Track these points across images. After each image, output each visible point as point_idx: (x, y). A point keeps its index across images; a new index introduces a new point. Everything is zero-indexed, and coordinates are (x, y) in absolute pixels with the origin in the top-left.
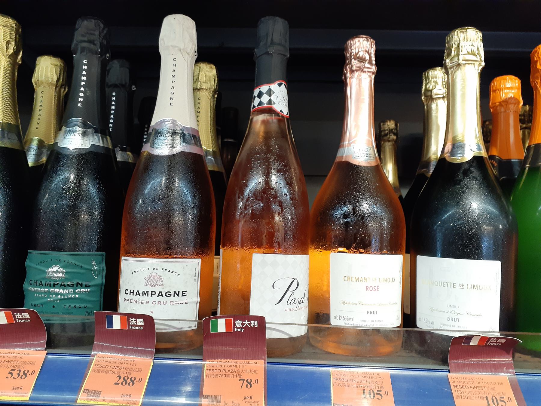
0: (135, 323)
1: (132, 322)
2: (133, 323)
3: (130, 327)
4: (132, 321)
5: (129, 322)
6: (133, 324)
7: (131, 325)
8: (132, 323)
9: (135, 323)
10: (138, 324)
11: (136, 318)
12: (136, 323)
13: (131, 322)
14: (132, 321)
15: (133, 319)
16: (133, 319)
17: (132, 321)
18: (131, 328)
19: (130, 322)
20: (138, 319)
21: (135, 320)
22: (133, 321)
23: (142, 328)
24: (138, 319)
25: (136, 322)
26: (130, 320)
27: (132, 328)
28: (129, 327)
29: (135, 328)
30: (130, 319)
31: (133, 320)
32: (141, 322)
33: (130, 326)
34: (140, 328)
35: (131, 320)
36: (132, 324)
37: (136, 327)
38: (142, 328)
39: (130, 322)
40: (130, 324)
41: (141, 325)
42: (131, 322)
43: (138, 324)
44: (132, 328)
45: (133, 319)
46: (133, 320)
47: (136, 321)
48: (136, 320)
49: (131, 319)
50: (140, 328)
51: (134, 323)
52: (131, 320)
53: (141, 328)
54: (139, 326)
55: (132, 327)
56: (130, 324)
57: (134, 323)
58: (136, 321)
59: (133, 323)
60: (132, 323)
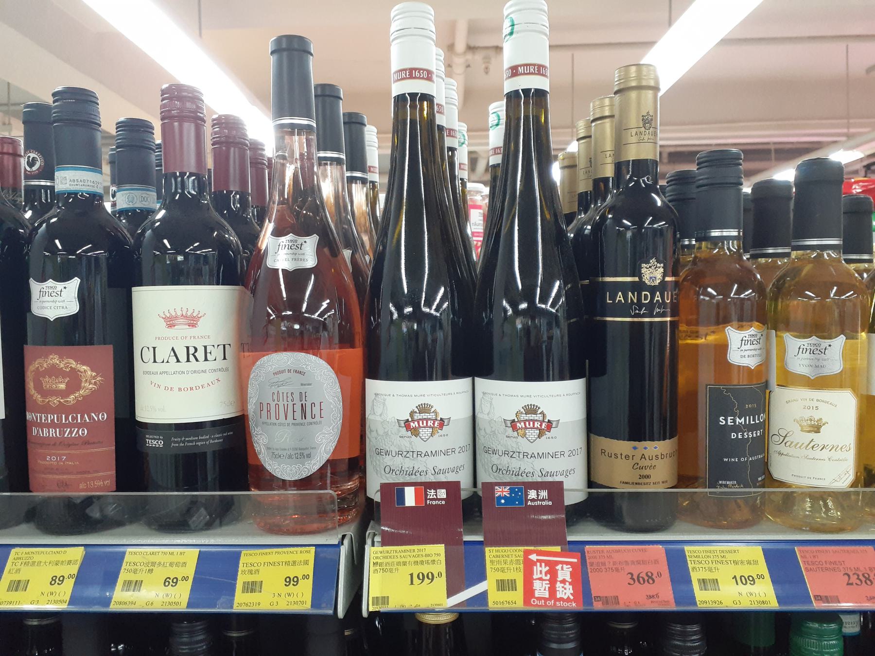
1: (430, 495)
2: (432, 496)
3: (428, 502)
5: (426, 495)
6: (431, 497)
7: (429, 499)
10: (438, 497)
11: (435, 489)
12: (436, 495)
14: (431, 493)
18: (429, 503)
19: (428, 494)
20: (438, 490)
21: (435, 491)
22: (432, 494)
23: (443, 502)
24: (438, 490)
26: (428, 493)
29: (434, 503)
30: (428, 490)
31: (431, 492)
32: (442, 493)
33: (428, 501)
35: (430, 492)
39: (428, 494)
40: (428, 498)
41: (442, 497)
43: (438, 497)
45: (432, 491)
46: (431, 492)
47: (435, 494)
48: (436, 492)
51: (433, 496)
52: (430, 492)
55: (431, 502)
57: (433, 496)
58: (435, 494)
59: (432, 496)
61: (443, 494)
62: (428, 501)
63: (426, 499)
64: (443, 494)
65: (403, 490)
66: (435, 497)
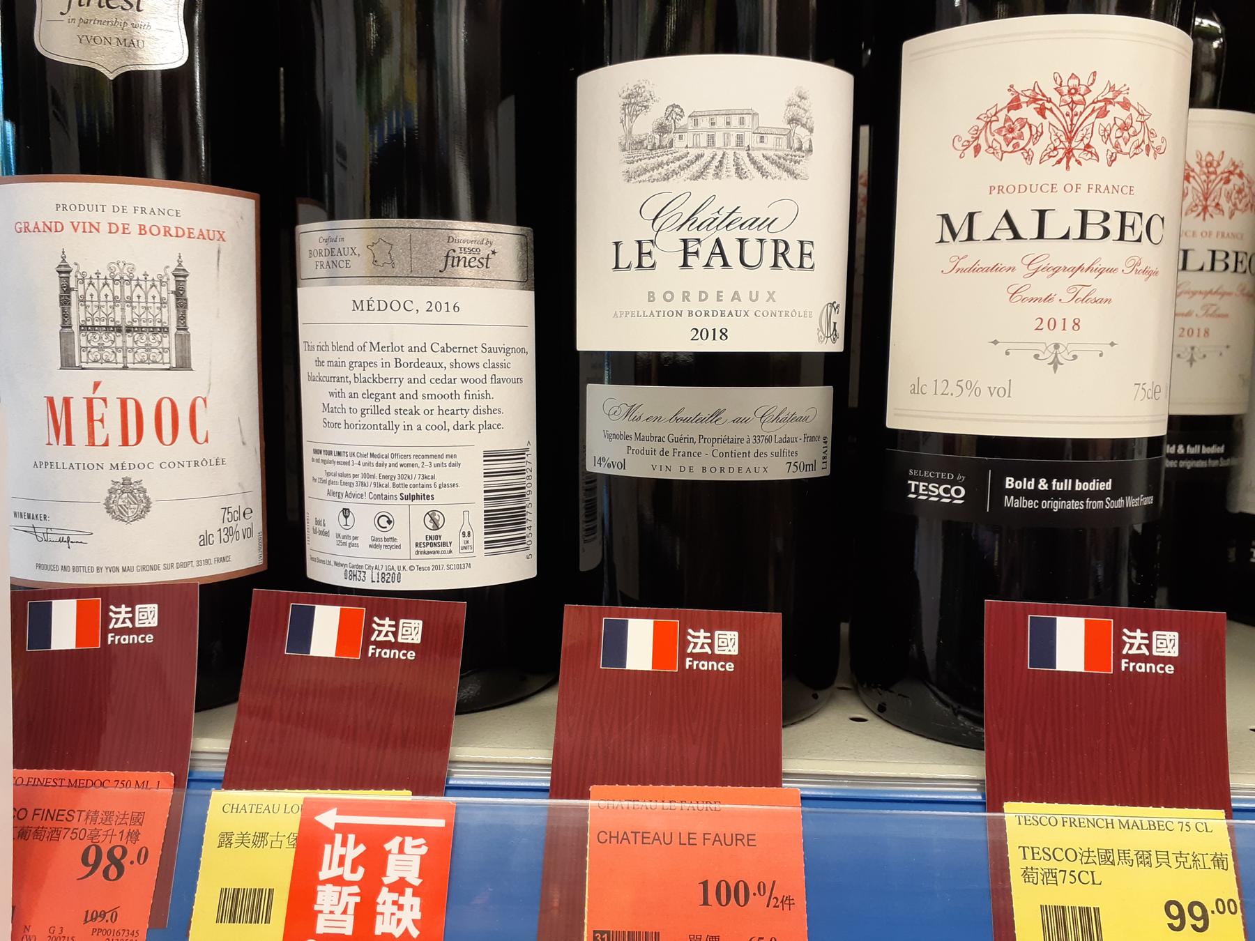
0: (1143, 647)
1: (1132, 645)
4: (1131, 641)
5: (1120, 644)
6: (1134, 651)
7: (1127, 656)
9: (1143, 647)
12: (1149, 647)
13: (1128, 646)
15: (1139, 630)
17: (1131, 641)
20: (1155, 633)
22: (1137, 642)
24: (1155, 633)
29: (1142, 668)
30: (1125, 631)
31: (1135, 638)
35: (1130, 637)
37: (1148, 665)
39: (1125, 643)
40: (1124, 652)
42: (1128, 646)
43: (1155, 653)
45: (1138, 633)
46: (1135, 638)
47: (1147, 642)
55: (1132, 664)
56: (1124, 652)
57: (1139, 648)
58: (1147, 642)
60: (1130, 648)
61: (1170, 645)
63: (1119, 656)
64: (1170, 645)
66: (1145, 651)
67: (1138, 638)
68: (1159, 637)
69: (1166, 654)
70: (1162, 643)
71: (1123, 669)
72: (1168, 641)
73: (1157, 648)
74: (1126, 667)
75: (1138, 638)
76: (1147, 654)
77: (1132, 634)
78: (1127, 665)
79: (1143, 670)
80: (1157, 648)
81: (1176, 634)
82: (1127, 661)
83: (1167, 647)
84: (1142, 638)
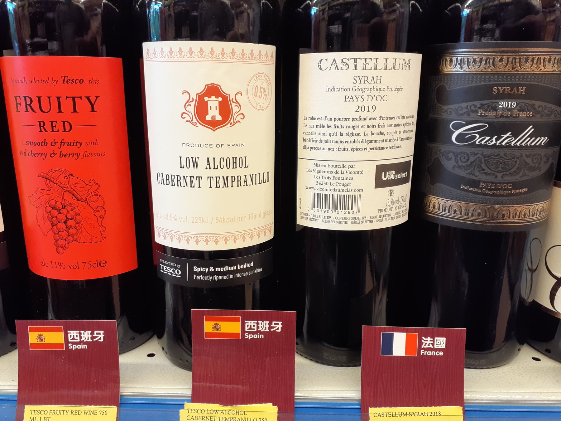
0: (430, 344)
1: (426, 344)
3: (422, 353)
4: (426, 342)
5: (421, 343)
6: (427, 346)
8: (425, 345)
11: (433, 337)
12: (433, 344)
13: (424, 344)
15: (429, 338)
16: (429, 338)
17: (426, 342)
19: (423, 343)
20: (436, 338)
21: (432, 339)
22: (428, 343)
23: (441, 353)
24: (436, 338)
25: (432, 344)
26: (423, 341)
27: (425, 354)
28: (419, 352)
29: (429, 353)
30: (423, 338)
31: (427, 341)
33: (422, 351)
34: (438, 353)
35: (425, 341)
36: (425, 347)
37: (432, 352)
38: (442, 353)
39: (423, 343)
40: (422, 347)
42: (424, 344)
43: (435, 347)
44: (425, 354)
45: (429, 339)
46: (427, 341)
47: (432, 342)
48: (433, 341)
49: (425, 338)
50: (438, 353)
51: (429, 345)
52: (425, 341)
53: (440, 354)
54: (436, 350)
56: (422, 347)
57: (429, 345)
58: (432, 342)
60: (425, 345)
61: (442, 343)
62: (422, 351)
63: (420, 349)
64: (442, 343)
65: (392, 335)
66: (431, 346)
67: (429, 341)
68: (437, 340)
69: (440, 347)
70: (438, 343)
71: (422, 354)
72: (441, 341)
73: (437, 344)
74: (423, 354)
75: (429, 341)
76: (432, 347)
77: (426, 339)
78: (423, 352)
79: (430, 354)
80: (437, 344)
81: (445, 339)
82: (423, 351)
83: (441, 344)
84: (430, 341)
